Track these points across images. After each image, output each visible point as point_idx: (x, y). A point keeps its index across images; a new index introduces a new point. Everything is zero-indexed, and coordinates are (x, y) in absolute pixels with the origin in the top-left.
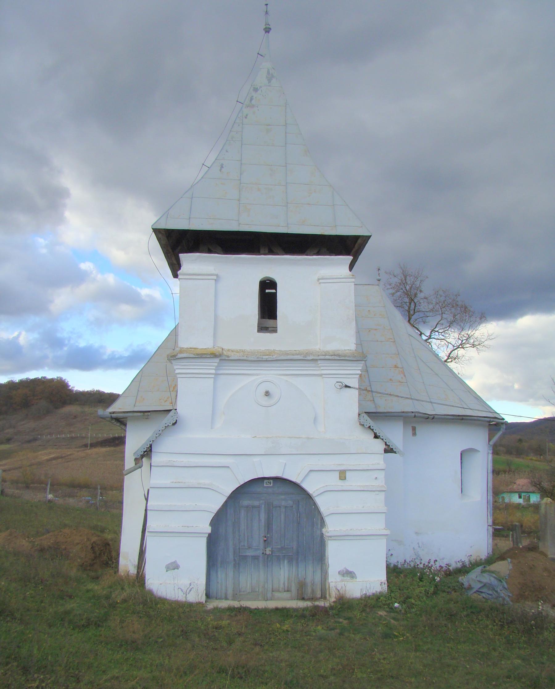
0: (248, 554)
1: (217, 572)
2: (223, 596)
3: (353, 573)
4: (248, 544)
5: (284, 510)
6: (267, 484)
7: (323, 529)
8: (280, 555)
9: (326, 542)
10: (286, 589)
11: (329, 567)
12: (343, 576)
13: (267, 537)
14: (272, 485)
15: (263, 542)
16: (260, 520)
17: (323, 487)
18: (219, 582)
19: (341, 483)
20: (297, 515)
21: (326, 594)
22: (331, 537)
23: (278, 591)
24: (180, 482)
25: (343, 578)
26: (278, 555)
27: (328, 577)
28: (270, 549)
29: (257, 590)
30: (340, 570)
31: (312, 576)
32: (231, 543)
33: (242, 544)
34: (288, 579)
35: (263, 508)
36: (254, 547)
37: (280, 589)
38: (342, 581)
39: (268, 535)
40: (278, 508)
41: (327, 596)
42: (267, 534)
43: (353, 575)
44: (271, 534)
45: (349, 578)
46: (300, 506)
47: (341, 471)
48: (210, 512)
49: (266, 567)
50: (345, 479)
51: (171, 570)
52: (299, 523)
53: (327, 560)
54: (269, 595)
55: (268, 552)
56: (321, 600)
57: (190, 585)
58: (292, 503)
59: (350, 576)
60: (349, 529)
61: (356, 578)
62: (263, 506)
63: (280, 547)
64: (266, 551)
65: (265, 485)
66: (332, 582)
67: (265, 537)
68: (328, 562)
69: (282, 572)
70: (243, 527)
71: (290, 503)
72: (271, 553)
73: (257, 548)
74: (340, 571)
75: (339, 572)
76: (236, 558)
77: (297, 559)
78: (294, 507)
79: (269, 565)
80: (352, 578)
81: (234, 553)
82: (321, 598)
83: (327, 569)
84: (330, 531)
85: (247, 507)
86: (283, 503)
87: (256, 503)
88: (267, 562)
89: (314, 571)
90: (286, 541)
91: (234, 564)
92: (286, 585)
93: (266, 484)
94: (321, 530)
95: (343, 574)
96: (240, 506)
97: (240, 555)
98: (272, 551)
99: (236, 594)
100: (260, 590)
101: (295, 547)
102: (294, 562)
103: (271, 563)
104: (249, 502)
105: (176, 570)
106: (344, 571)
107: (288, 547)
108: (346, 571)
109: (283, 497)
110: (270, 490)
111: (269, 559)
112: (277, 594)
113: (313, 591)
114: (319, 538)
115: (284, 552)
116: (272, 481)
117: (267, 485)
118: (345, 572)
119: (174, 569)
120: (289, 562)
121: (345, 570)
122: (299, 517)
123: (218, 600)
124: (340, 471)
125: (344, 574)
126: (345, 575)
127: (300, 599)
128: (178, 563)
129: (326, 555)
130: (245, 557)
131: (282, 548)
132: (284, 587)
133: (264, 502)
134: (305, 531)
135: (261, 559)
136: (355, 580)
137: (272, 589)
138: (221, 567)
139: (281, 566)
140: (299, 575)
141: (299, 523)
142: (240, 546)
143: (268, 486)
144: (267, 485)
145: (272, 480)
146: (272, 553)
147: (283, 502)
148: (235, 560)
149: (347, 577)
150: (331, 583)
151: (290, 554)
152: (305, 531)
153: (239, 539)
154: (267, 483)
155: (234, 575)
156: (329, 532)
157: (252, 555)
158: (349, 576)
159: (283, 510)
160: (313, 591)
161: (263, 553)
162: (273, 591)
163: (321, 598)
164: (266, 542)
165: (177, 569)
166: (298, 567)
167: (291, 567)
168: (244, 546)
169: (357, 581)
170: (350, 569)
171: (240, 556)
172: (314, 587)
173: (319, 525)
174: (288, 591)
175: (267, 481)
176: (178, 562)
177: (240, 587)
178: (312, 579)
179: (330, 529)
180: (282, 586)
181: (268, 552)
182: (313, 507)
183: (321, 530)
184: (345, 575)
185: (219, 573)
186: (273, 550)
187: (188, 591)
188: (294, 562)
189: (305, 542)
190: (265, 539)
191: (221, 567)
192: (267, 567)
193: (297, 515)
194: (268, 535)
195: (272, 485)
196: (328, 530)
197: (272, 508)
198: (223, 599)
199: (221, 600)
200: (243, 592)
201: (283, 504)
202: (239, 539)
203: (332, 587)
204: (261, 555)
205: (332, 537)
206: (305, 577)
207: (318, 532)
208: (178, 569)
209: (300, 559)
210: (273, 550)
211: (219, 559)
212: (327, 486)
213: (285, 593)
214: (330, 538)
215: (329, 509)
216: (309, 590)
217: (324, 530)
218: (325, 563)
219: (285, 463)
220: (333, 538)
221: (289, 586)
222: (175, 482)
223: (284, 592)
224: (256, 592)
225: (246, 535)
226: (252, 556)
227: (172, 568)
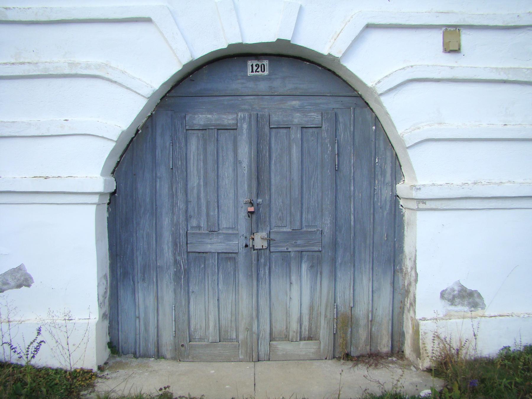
0: (208, 248)
1: (134, 293)
2: (152, 349)
3: (476, 295)
4: (208, 222)
5: (299, 136)
6: (254, 71)
7: (397, 185)
8: (290, 250)
9: (406, 218)
10: (305, 333)
11: (416, 281)
12: (452, 304)
13: (255, 205)
14: (266, 73)
15: (247, 217)
16: (237, 162)
17: (404, 68)
18: (139, 317)
19: (450, 60)
20: (333, 148)
21: (403, 343)
22: (423, 201)
23: (286, 338)
24: (24, 63)
25: (452, 308)
26: (284, 249)
27: (413, 304)
28: (264, 234)
29: (234, 336)
30: (445, 289)
31: (371, 302)
32: (166, 221)
33: (194, 222)
34: (311, 308)
35: (245, 131)
36: (224, 231)
37: (291, 334)
38: (448, 316)
39: (260, 200)
40: (285, 131)
41: (408, 350)
42: (257, 198)
43: (477, 300)
44: (267, 197)
45: (466, 309)
46: (341, 127)
47: (449, 29)
48: (103, 137)
49: (255, 283)
50: (459, 49)
51: (12, 288)
52: (337, 170)
53: (408, 264)
54: (264, 349)
55: (259, 242)
56: (393, 362)
57: (39, 333)
58: (320, 117)
59: (469, 304)
60: (469, 182)
61: (483, 308)
62: (245, 126)
63: (288, 230)
64: (253, 239)
65: (249, 73)
66: (424, 319)
67: (252, 204)
68: (414, 267)
69: (295, 288)
70: (194, 181)
71: (315, 118)
72: (265, 244)
73: (230, 232)
74: (446, 290)
75: (443, 295)
76: (178, 258)
77: (334, 260)
78: (324, 127)
79: (262, 273)
80: (473, 309)
81: (175, 244)
82: (392, 353)
83: (410, 284)
84: (424, 185)
85: (204, 129)
86: (297, 118)
87: (228, 119)
88: (258, 270)
89: (374, 289)
90: (304, 216)
91: (176, 273)
92: (306, 323)
93: (252, 71)
94: (393, 189)
95: (451, 297)
96: (187, 128)
97: (188, 251)
98: (269, 241)
99: (182, 345)
100: (241, 337)
101: (326, 230)
102: (326, 269)
103: (267, 272)
104: (209, 116)
105: (24, 288)
106: (454, 291)
107: (309, 230)
108: (460, 291)
109: (296, 103)
110: (263, 86)
111: (262, 260)
112: (282, 347)
113: (371, 337)
114: (388, 207)
115: (299, 242)
116: (266, 62)
117: (254, 73)
118: (456, 292)
119: (19, 286)
120: (312, 267)
121: (456, 288)
122: (338, 154)
123: (140, 360)
124: (446, 29)
125: (454, 297)
126: (457, 300)
127: (339, 359)
128: (29, 271)
129: (407, 248)
130: (202, 256)
131: (295, 234)
132: (301, 328)
133: (247, 115)
134: (352, 188)
135: (241, 259)
136: (480, 312)
137: (271, 334)
138: (144, 280)
139: (293, 278)
140: (338, 300)
141: (337, 170)
142: (189, 228)
146: (269, 245)
147: (298, 114)
148: (176, 262)
149: (463, 305)
150: (421, 323)
151: (316, 249)
152: (352, 188)
153: (186, 211)
154: (255, 68)
155: (175, 299)
157: (220, 251)
158: (466, 303)
159: (296, 134)
160: (371, 337)
161: (246, 246)
162: (272, 339)
163: (392, 353)
164: (254, 217)
165: (26, 286)
166: (335, 280)
167: (319, 275)
168: (199, 227)
169: (486, 314)
170: (470, 286)
171: (188, 253)
172: (373, 329)
173: (388, 178)
174: (310, 338)
175: (255, 63)
176: (29, 271)
177: (192, 329)
178: (370, 309)
179: (420, 182)
180: (294, 326)
181: (259, 242)
182: (374, 128)
183: (392, 186)
184: (457, 300)
185: (140, 295)
186: (272, 236)
187: (32, 349)
188: (326, 269)
189: (352, 217)
190: (252, 209)
191: (144, 280)
192: (258, 281)
193: (333, 148)
194: (260, 200)
195: (266, 73)
196: (416, 184)
197: (267, 129)
198: (149, 357)
199: (145, 360)
200: (201, 339)
201: (296, 121)
202: (186, 211)
203: (425, 333)
204: (242, 251)
205: (427, 202)
206: (352, 305)
207: (386, 193)
208: (29, 286)
209: (339, 260)
210: (272, 236)
211: (139, 261)
212: (412, 66)
213: (302, 342)
214: (421, 206)
215: (419, 128)
216: (362, 334)
217: (401, 189)
218: (401, 269)
219: (301, 8)
220: (429, 205)
221: (314, 329)
222: (13, 61)
223: (300, 340)
224: (231, 340)
225: (203, 202)
226: (218, 253)
227: (13, 283)
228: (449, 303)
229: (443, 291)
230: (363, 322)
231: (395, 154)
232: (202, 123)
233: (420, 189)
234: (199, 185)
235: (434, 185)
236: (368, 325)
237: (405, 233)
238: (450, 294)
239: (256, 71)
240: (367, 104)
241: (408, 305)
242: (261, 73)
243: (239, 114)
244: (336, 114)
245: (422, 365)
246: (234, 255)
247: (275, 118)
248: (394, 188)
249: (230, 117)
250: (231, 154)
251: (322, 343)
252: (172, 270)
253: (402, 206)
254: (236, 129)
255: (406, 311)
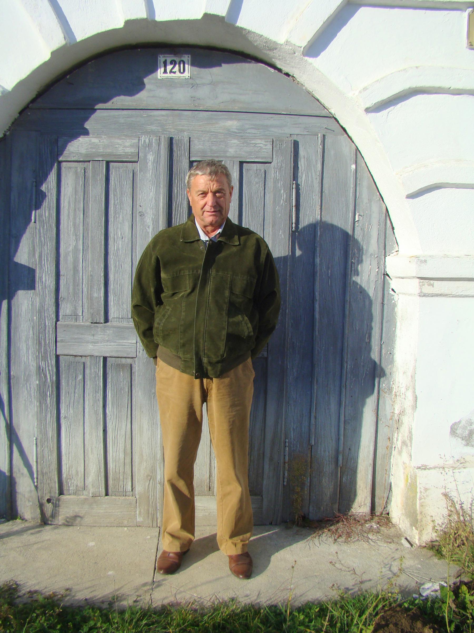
6: (168, 71)
12: (467, 445)
30: (457, 420)
62: (151, 157)
74: (460, 422)
75: (453, 431)
83: (402, 412)
93: (165, 72)
100: (138, 489)
117: (168, 75)
143: (172, 79)
144: (168, 75)
145: (186, 53)
147: (235, 141)
156: (425, 261)
168: (75, 316)
203: (426, 489)
228: (464, 442)
229: (455, 424)
230: (328, 468)
231: (385, 209)
232: (83, 151)
233: (425, 261)
234: (76, 249)
235: (446, 256)
236: (337, 473)
237: (398, 332)
238: (464, 428)
239: (171, 72)
240: (344, 130)
241: (398, 444)
242: (178, 74)
243: (143, 138)
244: (296, 144)
245: (420, 539)
246: (129, 361)
247: (197, 146)
248: (382, 263)
249: (128, 142)
250: (128, 200)
251: (265, 500)
252: (35, 382)
253: (393, 290)
254: (137, 162)
255: (394, 453)
